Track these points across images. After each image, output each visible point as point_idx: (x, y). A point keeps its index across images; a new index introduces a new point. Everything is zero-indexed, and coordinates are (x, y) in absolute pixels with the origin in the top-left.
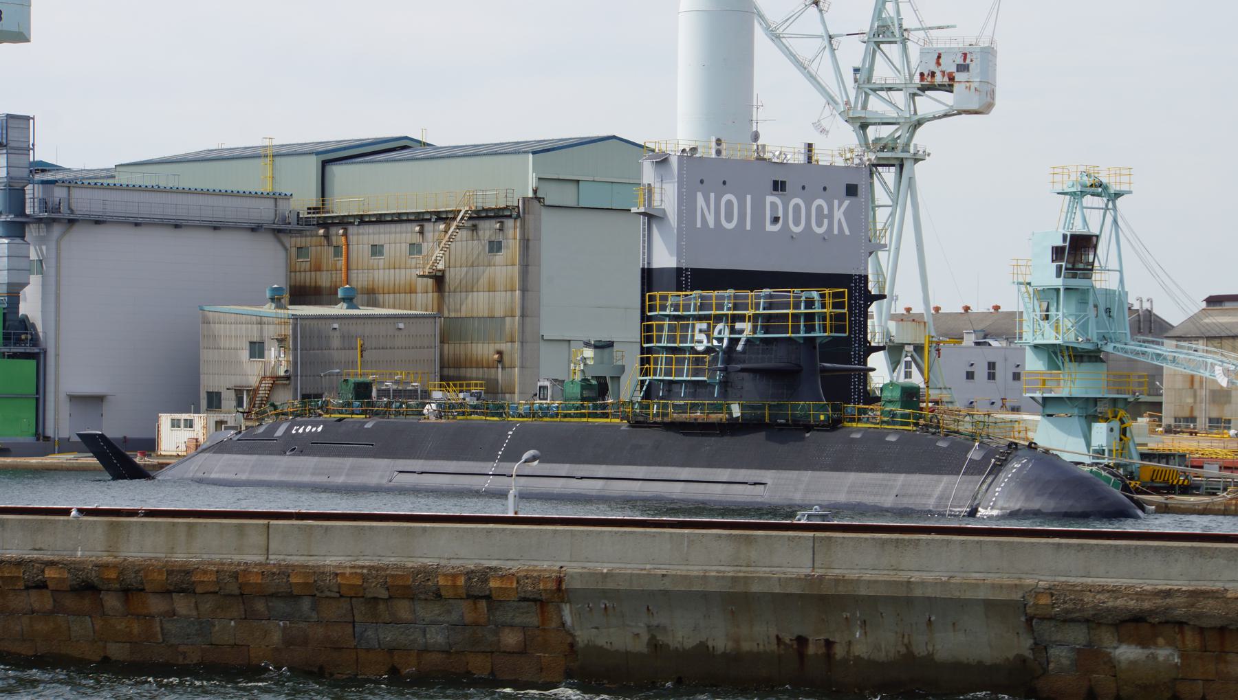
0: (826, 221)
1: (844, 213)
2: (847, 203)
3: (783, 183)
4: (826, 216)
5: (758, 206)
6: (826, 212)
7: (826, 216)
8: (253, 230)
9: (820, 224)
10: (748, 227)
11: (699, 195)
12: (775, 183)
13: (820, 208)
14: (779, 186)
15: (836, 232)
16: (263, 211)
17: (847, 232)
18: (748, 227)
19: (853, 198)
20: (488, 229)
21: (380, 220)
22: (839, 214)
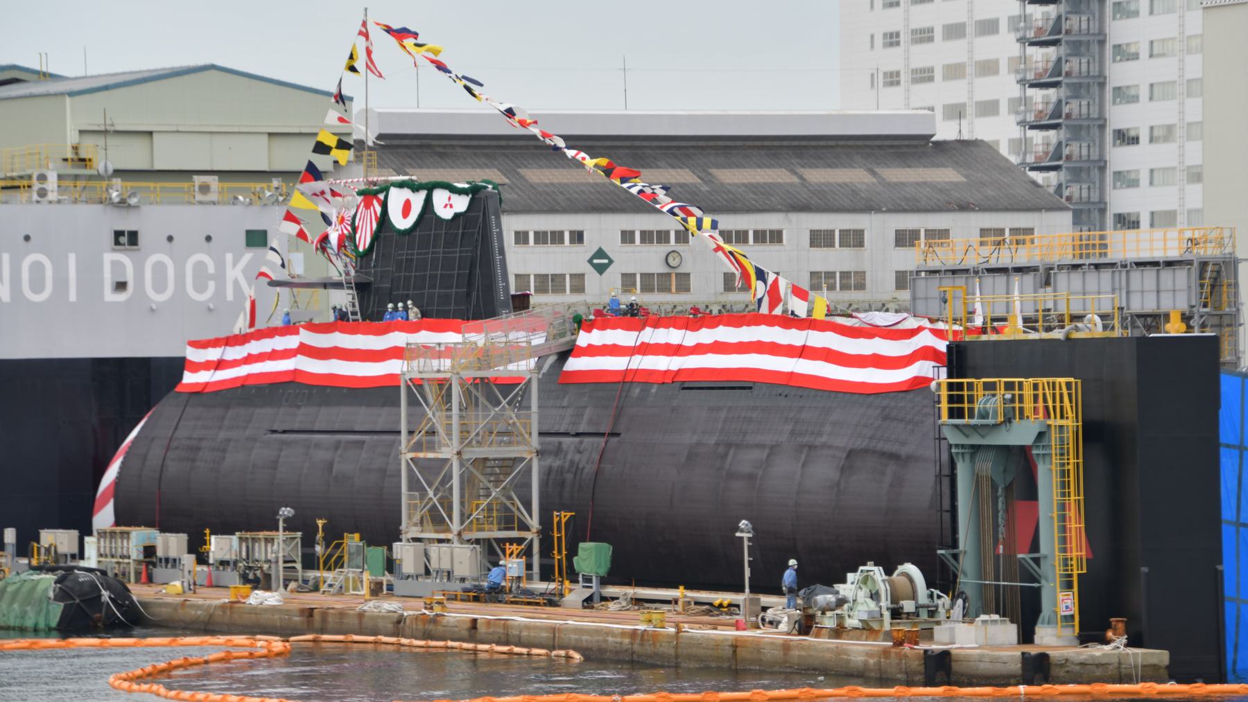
1: (244, 271)
2: (249, 255)
5: (90, 270)
10: (73, 297)
13: (200, 266)
18: (73, 297)
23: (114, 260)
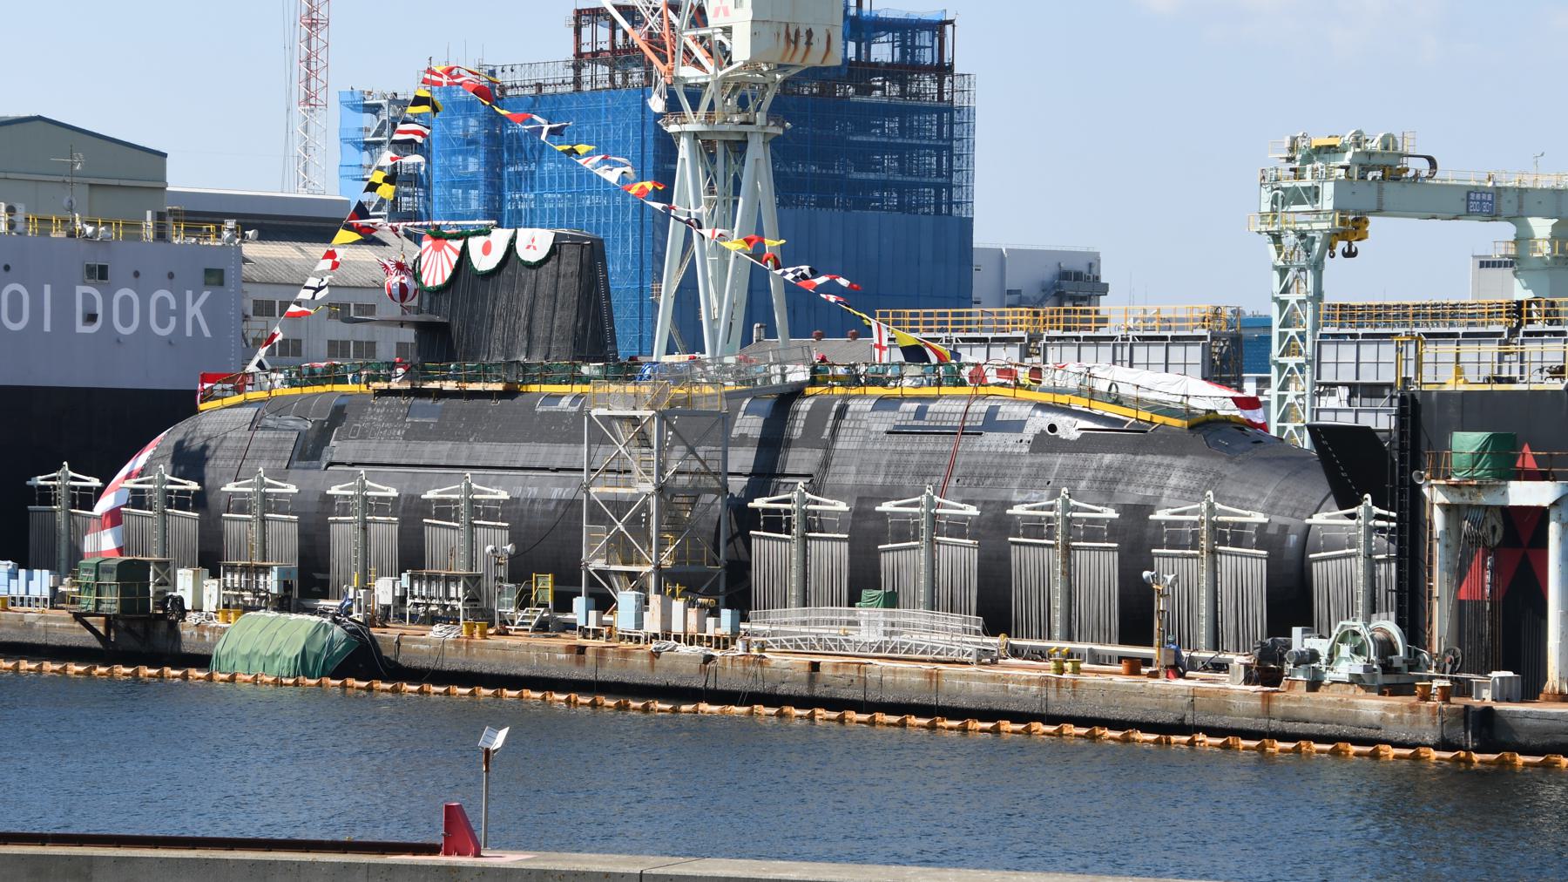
0: (173, 320)
4: (173, 313)
6: (173, 306)
7: (173, 313)
9: (163, 323)
10: (47, 328)
13: (163, 302)
14: (99, 273)
15: (189, 333)
17: (207, 333)
18: (47, 328)
19: (218, 289)
22: (194, 310)
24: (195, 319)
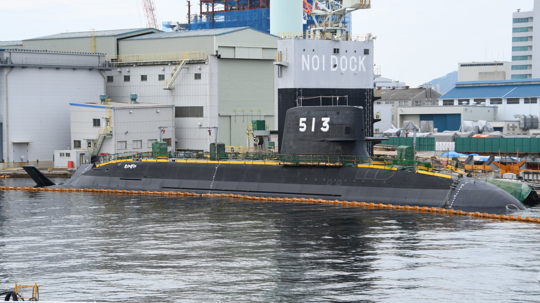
0: (356, 66)
1: (363, 62)
2: (364, 57)
3: (338, 50)
4: (356, 64)
5: (328, 60)
6: (356, 62)
7: (356, 64)
8: (90, 70)
9: (353, 67)
10: (324, 69)
11: (303, 56)
12: (335, 49)
13: (353, 60)
14: (336, 51)
15: (360, 70)
16: (94, 62)
17: (365, 70)
18: (324, 69)
20: (195, 69)
21: (145, 65)
22: (361, 63)
23: (333, 57)
24: (361, 65)
